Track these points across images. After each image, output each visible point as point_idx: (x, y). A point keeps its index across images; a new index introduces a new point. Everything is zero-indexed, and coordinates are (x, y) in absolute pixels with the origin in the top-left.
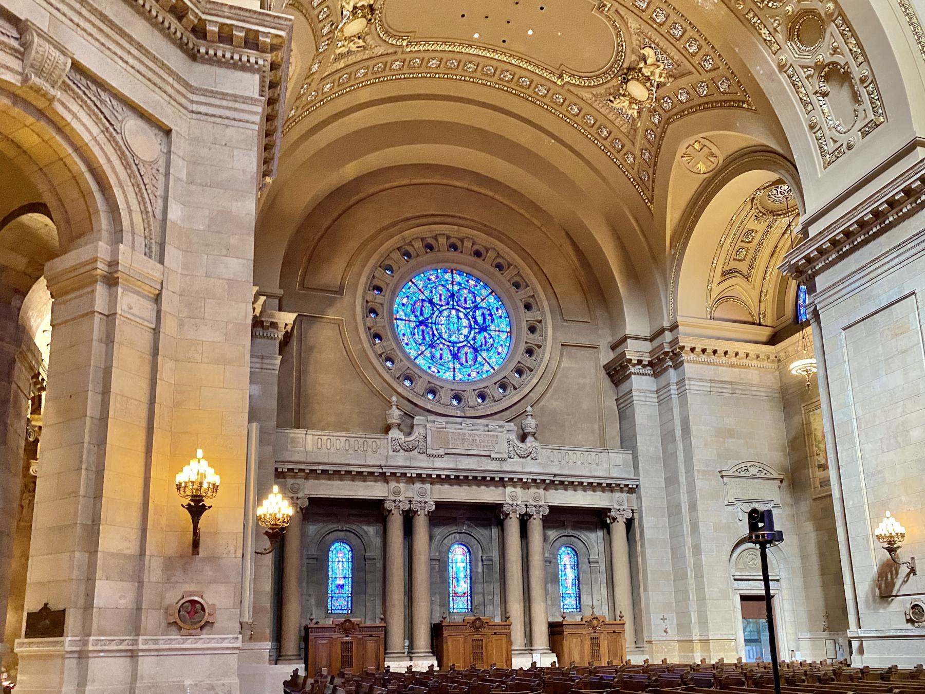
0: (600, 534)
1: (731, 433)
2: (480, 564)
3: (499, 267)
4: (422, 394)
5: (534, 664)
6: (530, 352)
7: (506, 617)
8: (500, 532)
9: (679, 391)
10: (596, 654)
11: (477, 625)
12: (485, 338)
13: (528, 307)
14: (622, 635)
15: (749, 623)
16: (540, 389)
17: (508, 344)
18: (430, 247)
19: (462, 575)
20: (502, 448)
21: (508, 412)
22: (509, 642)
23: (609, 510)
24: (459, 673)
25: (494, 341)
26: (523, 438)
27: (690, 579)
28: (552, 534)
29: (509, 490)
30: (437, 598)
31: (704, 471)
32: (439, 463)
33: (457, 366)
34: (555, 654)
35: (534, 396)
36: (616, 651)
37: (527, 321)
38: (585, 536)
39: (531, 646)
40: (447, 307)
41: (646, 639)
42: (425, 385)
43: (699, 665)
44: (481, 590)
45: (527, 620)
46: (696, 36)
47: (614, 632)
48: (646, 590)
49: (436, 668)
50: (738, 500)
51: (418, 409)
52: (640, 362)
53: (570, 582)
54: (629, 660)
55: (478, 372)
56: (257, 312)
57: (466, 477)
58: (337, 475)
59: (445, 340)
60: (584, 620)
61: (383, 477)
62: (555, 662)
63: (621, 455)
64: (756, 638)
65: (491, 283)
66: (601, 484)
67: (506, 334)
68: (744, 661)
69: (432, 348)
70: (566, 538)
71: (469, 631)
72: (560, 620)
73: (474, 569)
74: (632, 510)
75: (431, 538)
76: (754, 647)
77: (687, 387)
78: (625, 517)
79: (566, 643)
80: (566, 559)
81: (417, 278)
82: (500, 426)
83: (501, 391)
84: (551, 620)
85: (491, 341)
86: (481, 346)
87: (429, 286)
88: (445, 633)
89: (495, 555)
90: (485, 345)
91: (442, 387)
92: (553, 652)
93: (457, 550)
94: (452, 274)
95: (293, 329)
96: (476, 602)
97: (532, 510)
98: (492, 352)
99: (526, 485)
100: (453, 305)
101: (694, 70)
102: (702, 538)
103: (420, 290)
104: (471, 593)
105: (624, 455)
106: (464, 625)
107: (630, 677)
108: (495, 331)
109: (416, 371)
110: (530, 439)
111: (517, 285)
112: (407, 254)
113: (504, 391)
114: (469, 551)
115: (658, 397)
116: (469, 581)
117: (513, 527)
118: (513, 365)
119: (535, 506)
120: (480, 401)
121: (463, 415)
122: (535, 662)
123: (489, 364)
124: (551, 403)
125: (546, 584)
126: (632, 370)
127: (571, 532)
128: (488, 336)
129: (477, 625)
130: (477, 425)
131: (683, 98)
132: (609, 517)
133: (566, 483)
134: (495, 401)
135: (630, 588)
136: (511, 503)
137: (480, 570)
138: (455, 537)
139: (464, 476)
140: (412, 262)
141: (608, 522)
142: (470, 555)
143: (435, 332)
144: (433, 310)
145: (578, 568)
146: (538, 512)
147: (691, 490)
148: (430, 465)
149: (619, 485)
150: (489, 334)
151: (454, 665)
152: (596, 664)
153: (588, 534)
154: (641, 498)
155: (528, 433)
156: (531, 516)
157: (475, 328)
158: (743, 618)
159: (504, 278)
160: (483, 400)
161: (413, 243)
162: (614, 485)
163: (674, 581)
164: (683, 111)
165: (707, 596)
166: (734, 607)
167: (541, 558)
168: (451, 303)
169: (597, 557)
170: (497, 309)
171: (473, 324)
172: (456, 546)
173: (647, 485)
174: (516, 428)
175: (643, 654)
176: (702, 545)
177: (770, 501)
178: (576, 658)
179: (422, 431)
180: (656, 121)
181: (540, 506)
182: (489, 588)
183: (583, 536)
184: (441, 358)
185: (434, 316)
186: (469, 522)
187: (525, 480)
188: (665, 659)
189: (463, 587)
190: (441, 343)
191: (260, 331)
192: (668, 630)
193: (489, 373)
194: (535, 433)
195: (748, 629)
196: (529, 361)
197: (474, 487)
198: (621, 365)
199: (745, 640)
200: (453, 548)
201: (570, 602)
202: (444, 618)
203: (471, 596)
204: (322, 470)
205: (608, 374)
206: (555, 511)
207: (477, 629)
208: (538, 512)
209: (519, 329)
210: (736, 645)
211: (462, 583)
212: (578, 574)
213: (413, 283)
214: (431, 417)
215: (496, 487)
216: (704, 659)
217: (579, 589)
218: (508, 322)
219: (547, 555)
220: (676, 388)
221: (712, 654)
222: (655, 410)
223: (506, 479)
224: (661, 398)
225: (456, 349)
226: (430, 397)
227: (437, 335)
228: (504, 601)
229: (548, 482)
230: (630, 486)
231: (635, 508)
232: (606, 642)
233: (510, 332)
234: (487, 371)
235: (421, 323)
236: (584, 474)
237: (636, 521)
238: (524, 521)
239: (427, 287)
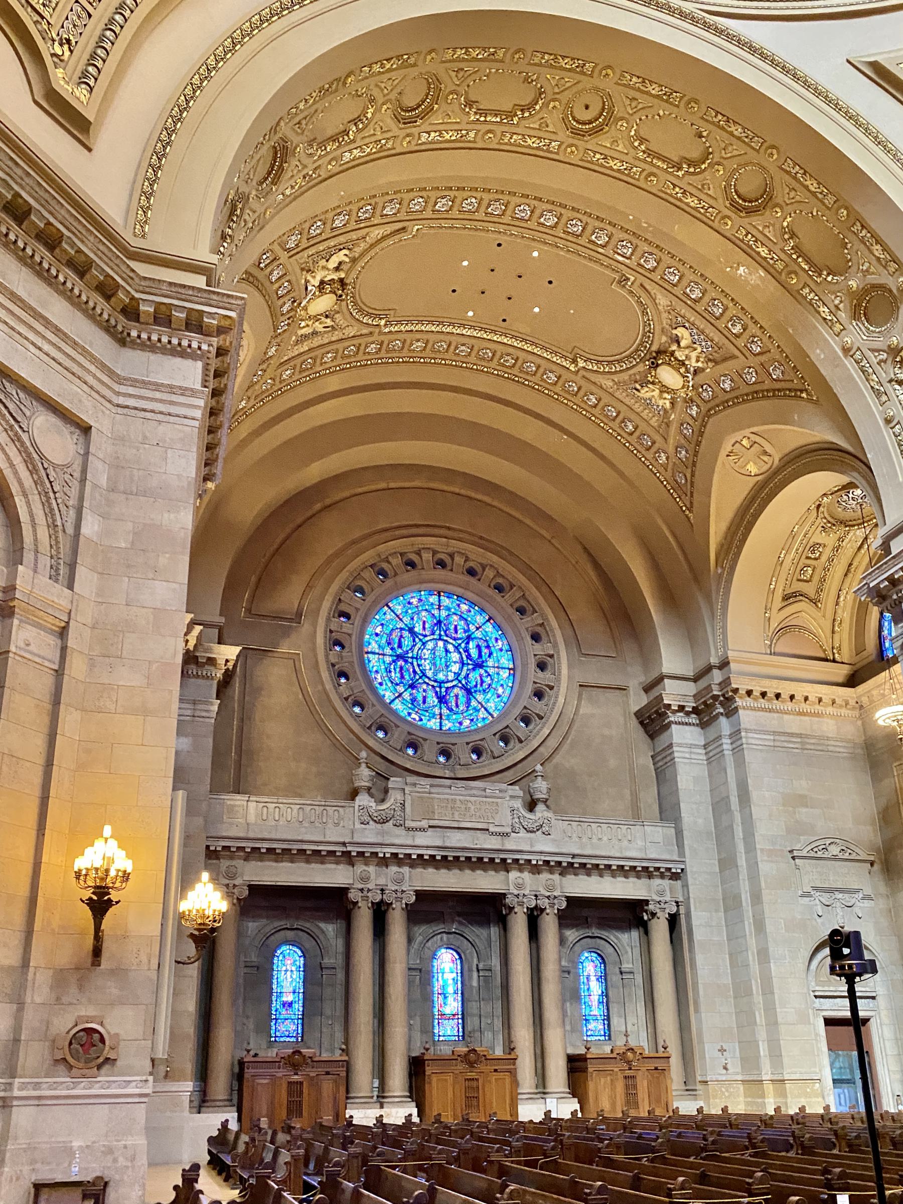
0: (635, 934)
1: (802, 801)
2: (475, 974)
3: (499, 588)
4: (399, 748)
5: (548, 1113)
6: (539, 694)
7: (510, 1048)
8: (502, 932)
9: (734, 746)
10: (631, 1098)
11: (471, 1059)
12: (481, 676)
13: (536, 637)
14: (666, 1072)
15: (838, 1056)
16: (552, 743)
17: (510, 685)
18: (411, 564)
19: (450, 989)
20: (504, 819)
21: (511, 771)
22: (515, 1083)
23: (646, 902)
24: (446, 1127)
25: (492, 679)
26: (531, 806)
27: (755, 996)
28: (572, 935)
29: (513, 875)
30: (417, 1022)
31: (770, 850)
32: (422, 839)
33: (445, 711)
34: (576, 1100)
35: (545, 751)
36: (659, 1093)
37: (535, 655)
39: (544, 1087)
40: (432, 637)
41: (699, 1078)
42: (404, 737)
43: (772, 1117)
44: (476, 1011)
45: (539, 1052)
47: (656, 1069)
48: (697, 1011)
49: (416, 1119)
50: (816, 889)
52: (681, 708)
53: (595, 998)
54: (677, 1108)
55: (472, 720)
56: (191, 646)
57: (457, 858)
59: (429, 679)
60: (616, 1052)
61: (348, 858)
62: (576, 1111)
63: (660, 829)
64: (849, 1077)
65: (487, 606)
66: (635, 867)
67: (507, 671)
68: (833, 1110)
69: (413, 689)
70: (588, 940)
71: (461, 1067)
72: (582, 1051)
73: (467, 982)
74: (677, 902)
75: (410, 940)
76: (846, 1090)
77: (744, 740)
78: (667, 911)
79: (591, 1085)
80: (589, 967)
81: (395, 602)
82: (500, 791)
83: (502, 744)
84: (570, 1051)
85: (488, 680)
86: (476, 686)
87: (410, 611)
88: (428, 1070)
89: (496, 963)
90: (481, 685)
91: (425, 740)
92: (574, 1097)
93: (444, 955)
94: (439, 596)
95: (235, 666)
96: (469, 1028)
97: (543, 903)
98: (489, 695)
99: (536, 869)
100: (440, 635)
102: (769, 939)
103: (397, 616)
104: (463, 1014)
106: (454, 1058)
107: (679, 1135)
108: (494, 667)
109: (392, 718)
110: (540, 807)
111: (522, 611)
112: (382, 572)
113: (506, 744)
114: (461, 958)
115: (706, 753)
116: (460, 999)
117: (519, 926)
118: (517, 711)
119: (548, 897)
120: (474, 757)
121: (452, 775)
122: (550, 1111)
123: (486, 709)
124: (567, 760)
125: (564, 1001)
126: (672, 719)
127: (596, 932)
128: (485, 674)
129: (471, 1059)
130: (472, 788)
132: (646, 911)
133: (589, 866)
134: (494, 758)
135: (676, 1008)
136: (516, 892)
137: (475, 983)
138: (441, 939)
139: (454, 857)
140: (389, 583)
141: (646, 918)
142: (461, 962)
143: (417, 669)
144: (414, 641)
145: (606, 980)
146: (552, 905)
147: (754, 877)
148: (409, 842)
149: (659, 868)
150: (486, 671)
151: (439, 1115)
152: (633, 1113)
154: (687, 886)
155: (538, 800)
156: (542, 910)
157: (468, 664)
158: (830, 1049)
159: (505, 601)
160: (479, 755)
161: (390, 559)
162: (651, 869)
163: (735, 998)
165: (780, 1020)
166: (817, 1035)
167: (557, 967)
168: (438, 632)
169: (631, 966)
170: (497, 640)
171: (465, 658)
172: (443, 950)
173: (695, 870)
174: (521, 793)
175: (696, 1100)
176: (771, 949)
177: (857, 891)
178: (605, 1104)
179: (399, 796)
181: (555, 897)
182: (486, 1008)
183: (612, 937)
184: (424, 702)
185: (416, 649)
186: (461, 919)
187: (534, 862)
188: (726, 1107)
189: (453, 1005)
190: (425, 682)
191: (193, 669)
192: (729, 1066)
193: (487, 722)
194: (547, 800)
195: (837, 1065)
196: (537, 706)
197: (468, 872)
198: (656, 712)
199: (834, 1081)
200: (439, 953)
201: (597, 1026)
202: (427, 1050)
203: (463, 1019)
205: (641, 723)
206: (573, 902)
207: (471, 1064)
208: (552, 905)
209: (525, 665)
210: (822, 1087)
211: (450, 999)
212: (606, 989)
213: (390, 608)
214: (411, 779)
215: (496, 871)
216: (779, 1107)
217: (608, 1009)
218: (510, 656)
219: (563, 963)
220: (729, 741)
221: (789, 1100)
222: (702, 771)
223: (509, 861)
224: (711, 754)
225: (443, 690)
226: (410, 752)
227: (419, 672)
228: (507, 1025)
229: (565, 864)
230: (674, 870)
231: (681, 899)
232: (645, 1083)
233: (513, 669)
234: (484, 719)
235: (399, 657)
236: (611, 854)
237: (683, 917)
238: (534, 917)
239: (407, 612)
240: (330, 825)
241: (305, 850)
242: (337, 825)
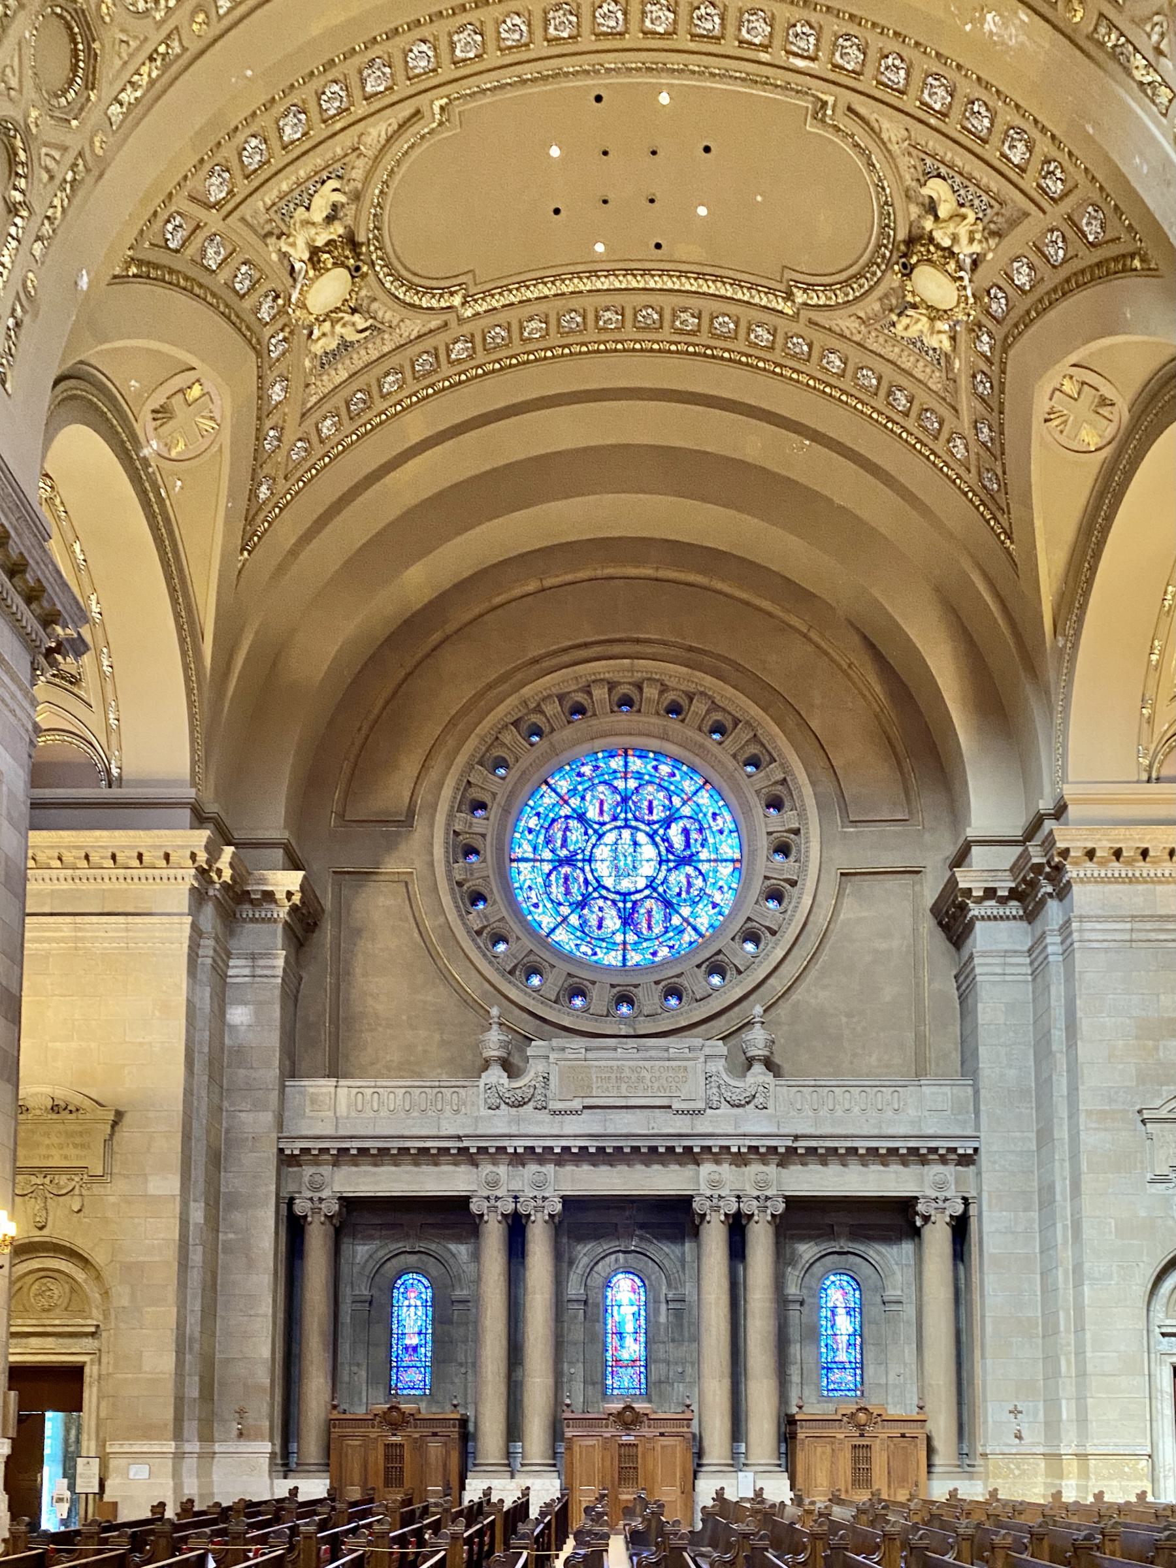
4: (553, 998)
16: (790, 970)
21: (724, 1018)
38: (879, 1253)
46: (1018, 121)
51: (547, 1027)
58: (382, 1156)
63: (947, 1089)
70: (836, 1256)
91: (594, 983)
101: (1032, 209)
105: (956, 1089)
109: (546, 955)
121: (632, 1033)
131: (1022, 279)
134: (697, 1001)
153: (883, 1249)
164: (1028, 312)
169: (899, 1293)
173: (995, 1148)
180: (986, 348)
183: (871, 1253)
200: (614, 1280)
204: (359, 1149)
240: (448, 1112)
241: (408, 1149)
242: (457, 1111)
